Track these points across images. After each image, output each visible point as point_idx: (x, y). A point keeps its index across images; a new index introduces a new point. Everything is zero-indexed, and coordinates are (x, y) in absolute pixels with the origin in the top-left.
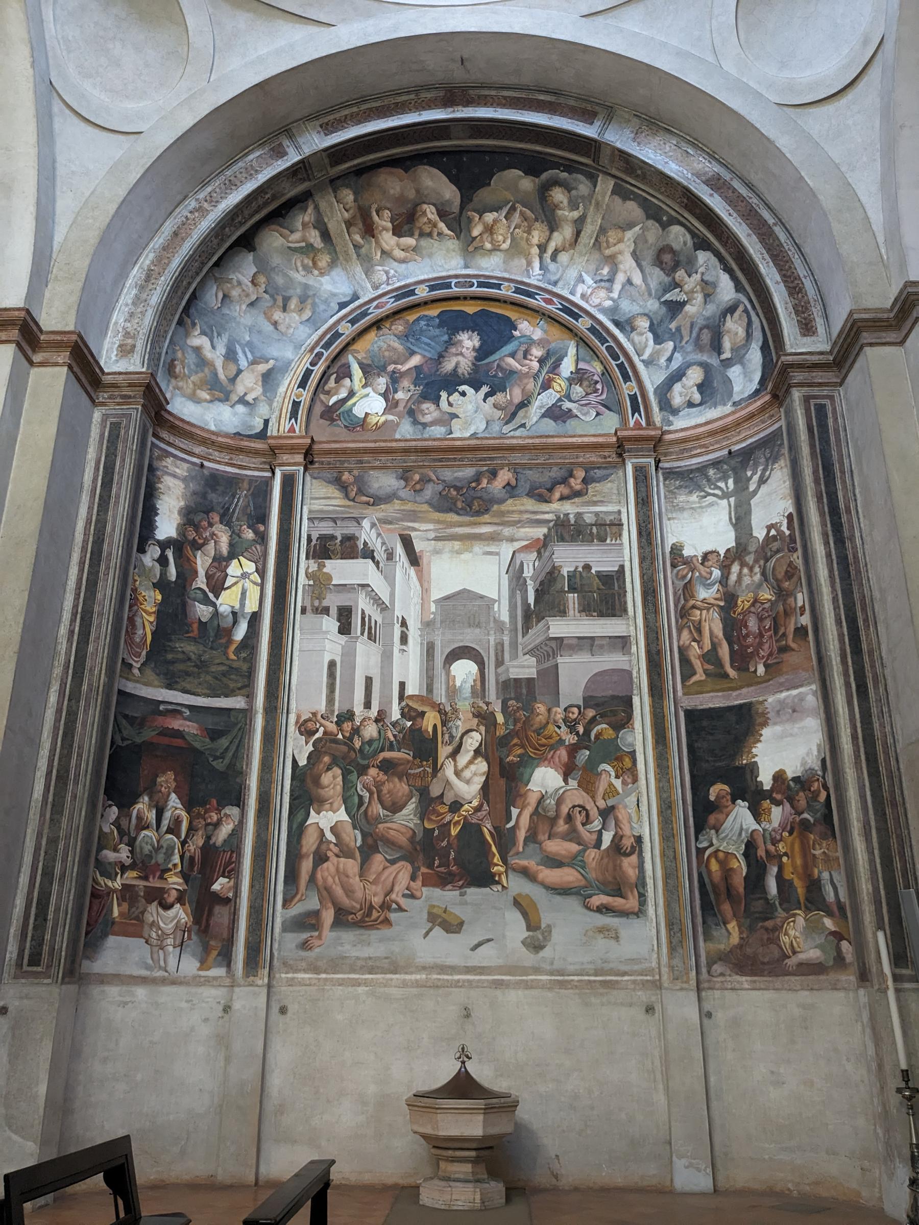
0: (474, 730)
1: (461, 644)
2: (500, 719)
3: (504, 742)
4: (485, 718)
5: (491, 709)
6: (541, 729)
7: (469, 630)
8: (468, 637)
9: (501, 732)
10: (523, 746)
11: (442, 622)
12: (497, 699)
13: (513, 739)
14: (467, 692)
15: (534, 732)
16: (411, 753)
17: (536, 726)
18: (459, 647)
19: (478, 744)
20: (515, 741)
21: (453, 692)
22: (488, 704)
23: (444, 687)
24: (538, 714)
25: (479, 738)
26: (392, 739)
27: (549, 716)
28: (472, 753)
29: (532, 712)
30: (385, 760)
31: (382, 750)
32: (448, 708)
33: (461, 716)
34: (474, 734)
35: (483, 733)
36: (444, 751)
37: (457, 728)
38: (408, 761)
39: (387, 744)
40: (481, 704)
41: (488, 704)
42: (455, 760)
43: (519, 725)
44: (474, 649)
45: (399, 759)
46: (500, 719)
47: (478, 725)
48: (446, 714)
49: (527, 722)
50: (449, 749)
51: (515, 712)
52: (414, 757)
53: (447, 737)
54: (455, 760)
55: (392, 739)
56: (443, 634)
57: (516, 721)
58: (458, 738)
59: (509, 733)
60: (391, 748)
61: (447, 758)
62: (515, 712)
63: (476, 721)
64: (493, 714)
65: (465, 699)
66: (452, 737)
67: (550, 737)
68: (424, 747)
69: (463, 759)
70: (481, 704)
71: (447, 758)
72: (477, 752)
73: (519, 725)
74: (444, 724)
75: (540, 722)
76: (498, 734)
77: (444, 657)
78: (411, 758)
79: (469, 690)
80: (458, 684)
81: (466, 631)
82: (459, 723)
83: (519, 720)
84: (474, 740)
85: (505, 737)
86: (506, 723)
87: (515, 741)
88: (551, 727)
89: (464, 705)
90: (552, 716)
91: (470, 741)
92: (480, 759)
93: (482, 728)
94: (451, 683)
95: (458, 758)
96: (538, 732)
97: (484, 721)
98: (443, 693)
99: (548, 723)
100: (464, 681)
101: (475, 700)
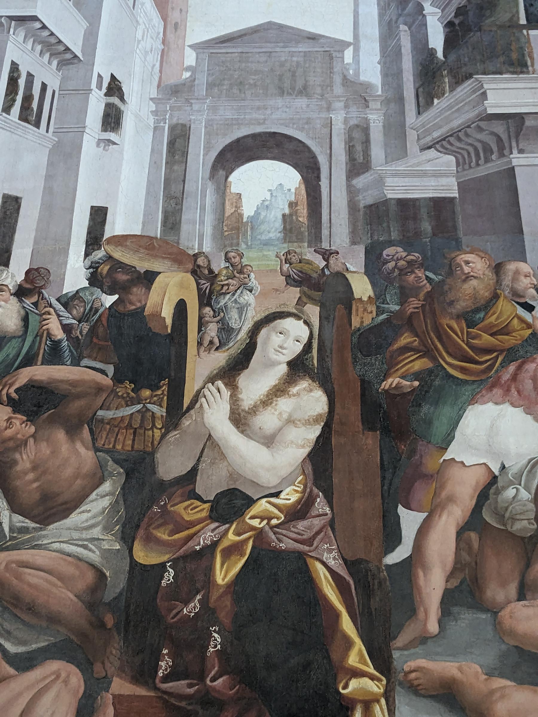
0: (289, 315)
1: (259, 129)
2: (362, 287)
3: (373, 343)
4: (321, 287)
5: (335, 265)
6: (477, 310)
7: (279, 102)
8: (279, 116)
9: (363, 318)
10: (427, 352)
11: (211, 86)
12: (353, 243)
13: (397, 336)
14: (272, 227)
15: (458, 317)
16: (110, 369)
17: (461, 305)
18: (254, 136)
19: (299, 348)
20: (406, 339)
21: (232, 228)
22: (327, 255)
23: (209, 219)
24: (468, 277)
25: (303, 332)
26: (59, 334)
27: (498, 282)
28: (283, 369)
29: (451, 272)
30: (33, 388)
31: (29, 361)
32: (219, 265)
33: (253, 282)
34: (289, 323)
35: (316, 322)
36: (201, 365)
37: (242, 309)
38: (99, 389)
39: (44, 347)
40: (310, 255)
41: (327, 255)
42: (232, 386)
43: (413, 304)
44: (290, 139)
45: (74, 384)
46: (362, 287)
47: (300, 303)
48: (212, 276)
49: (437, 297)
50: (219, 359)
51: (403, 273)
52: (118, 379)
53: (212, 331)
54: (232, 386)
55: (59, 334)
56: (214, 109)
57: (404, 294)
58: (243, 334)
59: (387, 321)
60: (54, 355)
61: (212, 380)
62: (403, 273)
63: (295, 293)
64: (341, 277)
65: (267, 243)
66: (226, 331)
67: (505, 331)
68: (145, 356)
69: (255, 385)
70: (310, 255)
71: (212, 380)
72: (298, 367)
73: (413, 304)
74: (206, 299)
75: (474, 297)
76: (356, 323)
77: (214, 154)
78: (107, 381)
79: (279, 224)
80: (248, 210)
81: (272, 103)
82: (248, 298)
83: (415, 290)
84: (289, 338)
85: (374, 329)
86: (379, 297)
87: (406, 339)
88: (505, 309)
89: (264, 259)
90: (507, 281)
91: (276, 340)
92: (304, 384)
93: (313, 312)
94: (229, 210)
95: (242, 380)
96: (470, 318)
97: (317, 295)
98: (208, 230)
99: (495, 297)
100: (265, 206)
101: (294, 247)
